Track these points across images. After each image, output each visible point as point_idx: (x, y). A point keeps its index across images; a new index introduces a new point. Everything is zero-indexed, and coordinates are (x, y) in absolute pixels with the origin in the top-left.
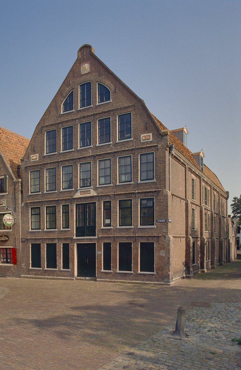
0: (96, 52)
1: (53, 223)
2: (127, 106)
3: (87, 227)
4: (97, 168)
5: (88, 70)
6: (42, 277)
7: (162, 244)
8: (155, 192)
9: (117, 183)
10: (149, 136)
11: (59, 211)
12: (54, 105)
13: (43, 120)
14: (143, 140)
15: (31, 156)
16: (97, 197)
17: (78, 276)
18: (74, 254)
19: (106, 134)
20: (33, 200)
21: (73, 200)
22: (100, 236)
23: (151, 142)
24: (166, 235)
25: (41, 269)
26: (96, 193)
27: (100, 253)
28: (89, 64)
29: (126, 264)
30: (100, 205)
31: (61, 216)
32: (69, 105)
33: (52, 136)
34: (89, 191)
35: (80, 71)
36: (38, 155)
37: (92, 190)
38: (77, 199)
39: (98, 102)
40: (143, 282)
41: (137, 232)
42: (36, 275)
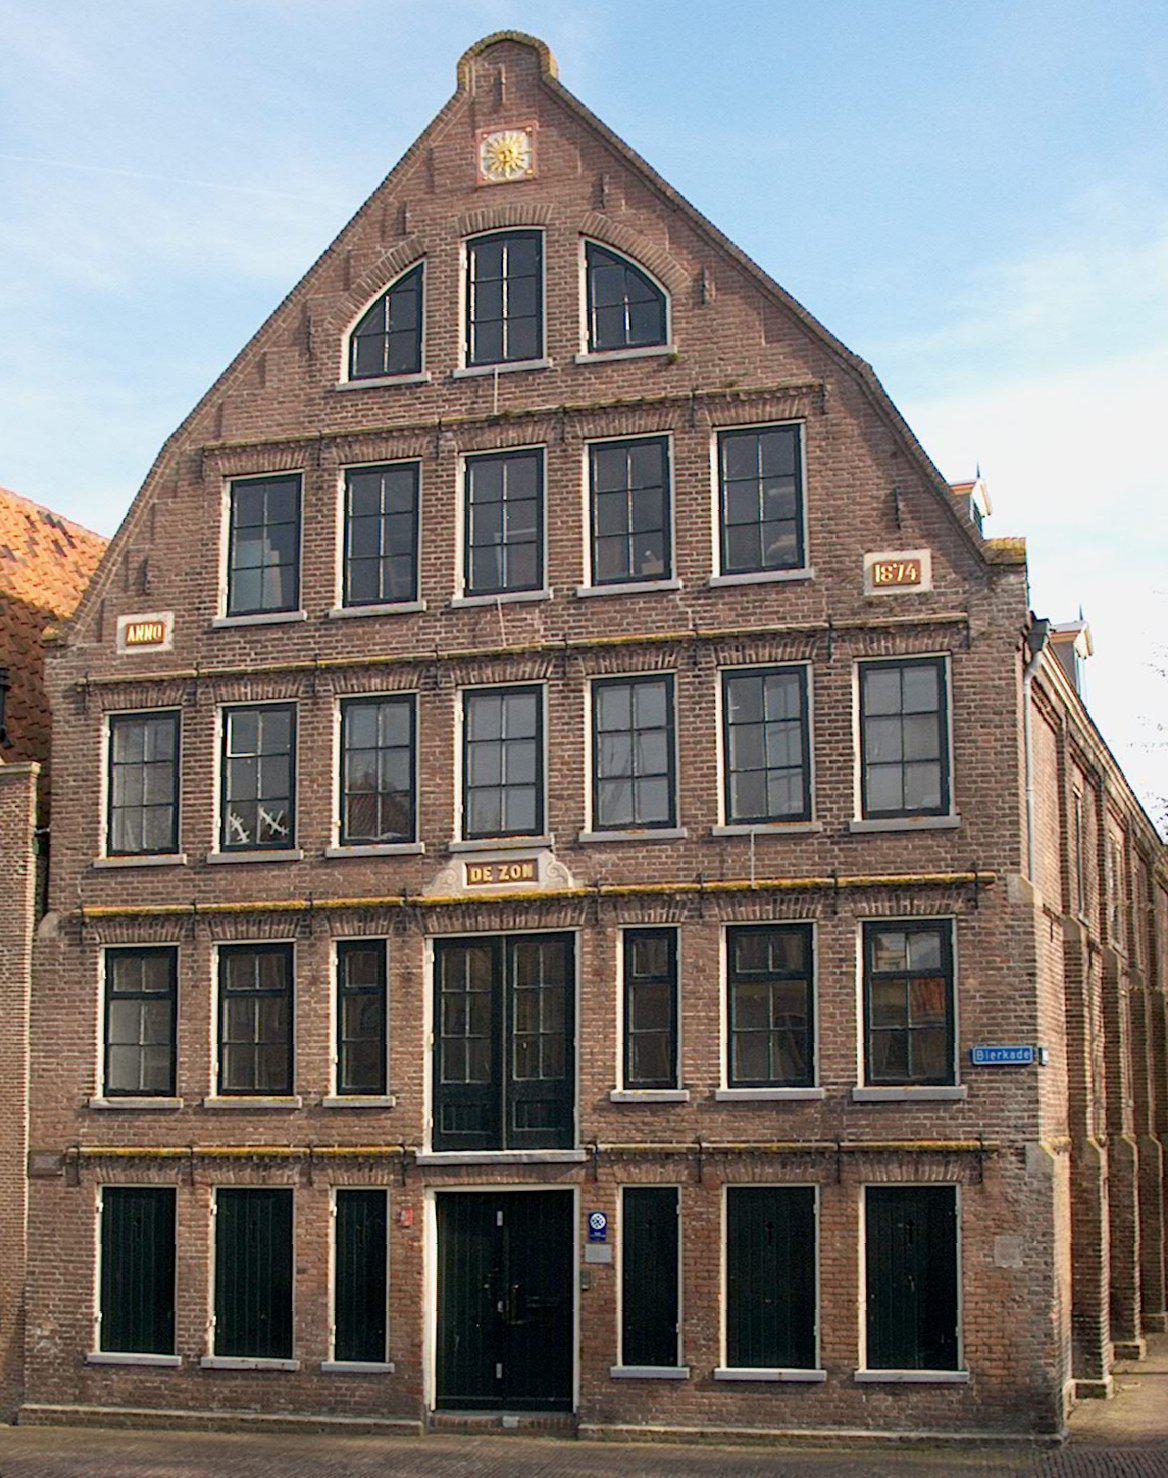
0: (571, 73)
1: (264, 1060)
2: (770, 384)
3: (505, 1082)
4: (580, 730)
5: (525, 165)
6: (181, 1413)
7: (1004, 1195)
8: (957, 888)
9: (716, 822)
10: (917, 563)
11: (318, 980)
12: (296, 326)
13: (215, 404)
14: (877, 586)
15: (123, 621)
16: (586, 903)
17: (441, 1404)
18: (421, 1265)
19: (641, 530)
20: (125, 902)
21: (410, 914)
22: (602, 1147)
23: (923, 597)
24: (1027, 1144)
25: (178, 1359)
26: (574, 875)
27: (600, 1257)
28: (529, 134)
29: (775, 1323)
30: (602, 948)
31: (327, 1016)
32: (396, 338)
33: (274, 508)
34: (526, 861)
35: (475, 166)
36: (169, 618)
37: (547, 861)
38: (451, 908)
39: (590, 342)
40: (887, 1434)
41: (848, 1126)
42: (138, 1404)
